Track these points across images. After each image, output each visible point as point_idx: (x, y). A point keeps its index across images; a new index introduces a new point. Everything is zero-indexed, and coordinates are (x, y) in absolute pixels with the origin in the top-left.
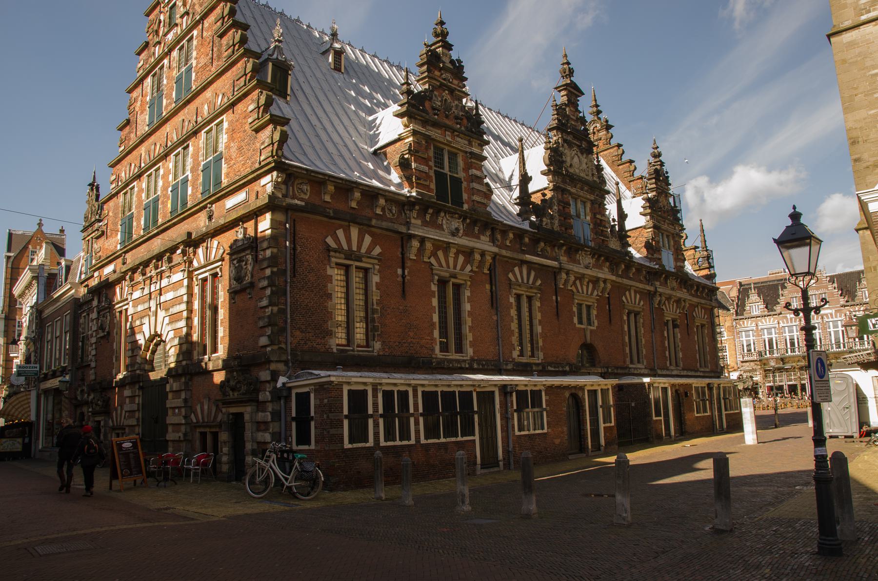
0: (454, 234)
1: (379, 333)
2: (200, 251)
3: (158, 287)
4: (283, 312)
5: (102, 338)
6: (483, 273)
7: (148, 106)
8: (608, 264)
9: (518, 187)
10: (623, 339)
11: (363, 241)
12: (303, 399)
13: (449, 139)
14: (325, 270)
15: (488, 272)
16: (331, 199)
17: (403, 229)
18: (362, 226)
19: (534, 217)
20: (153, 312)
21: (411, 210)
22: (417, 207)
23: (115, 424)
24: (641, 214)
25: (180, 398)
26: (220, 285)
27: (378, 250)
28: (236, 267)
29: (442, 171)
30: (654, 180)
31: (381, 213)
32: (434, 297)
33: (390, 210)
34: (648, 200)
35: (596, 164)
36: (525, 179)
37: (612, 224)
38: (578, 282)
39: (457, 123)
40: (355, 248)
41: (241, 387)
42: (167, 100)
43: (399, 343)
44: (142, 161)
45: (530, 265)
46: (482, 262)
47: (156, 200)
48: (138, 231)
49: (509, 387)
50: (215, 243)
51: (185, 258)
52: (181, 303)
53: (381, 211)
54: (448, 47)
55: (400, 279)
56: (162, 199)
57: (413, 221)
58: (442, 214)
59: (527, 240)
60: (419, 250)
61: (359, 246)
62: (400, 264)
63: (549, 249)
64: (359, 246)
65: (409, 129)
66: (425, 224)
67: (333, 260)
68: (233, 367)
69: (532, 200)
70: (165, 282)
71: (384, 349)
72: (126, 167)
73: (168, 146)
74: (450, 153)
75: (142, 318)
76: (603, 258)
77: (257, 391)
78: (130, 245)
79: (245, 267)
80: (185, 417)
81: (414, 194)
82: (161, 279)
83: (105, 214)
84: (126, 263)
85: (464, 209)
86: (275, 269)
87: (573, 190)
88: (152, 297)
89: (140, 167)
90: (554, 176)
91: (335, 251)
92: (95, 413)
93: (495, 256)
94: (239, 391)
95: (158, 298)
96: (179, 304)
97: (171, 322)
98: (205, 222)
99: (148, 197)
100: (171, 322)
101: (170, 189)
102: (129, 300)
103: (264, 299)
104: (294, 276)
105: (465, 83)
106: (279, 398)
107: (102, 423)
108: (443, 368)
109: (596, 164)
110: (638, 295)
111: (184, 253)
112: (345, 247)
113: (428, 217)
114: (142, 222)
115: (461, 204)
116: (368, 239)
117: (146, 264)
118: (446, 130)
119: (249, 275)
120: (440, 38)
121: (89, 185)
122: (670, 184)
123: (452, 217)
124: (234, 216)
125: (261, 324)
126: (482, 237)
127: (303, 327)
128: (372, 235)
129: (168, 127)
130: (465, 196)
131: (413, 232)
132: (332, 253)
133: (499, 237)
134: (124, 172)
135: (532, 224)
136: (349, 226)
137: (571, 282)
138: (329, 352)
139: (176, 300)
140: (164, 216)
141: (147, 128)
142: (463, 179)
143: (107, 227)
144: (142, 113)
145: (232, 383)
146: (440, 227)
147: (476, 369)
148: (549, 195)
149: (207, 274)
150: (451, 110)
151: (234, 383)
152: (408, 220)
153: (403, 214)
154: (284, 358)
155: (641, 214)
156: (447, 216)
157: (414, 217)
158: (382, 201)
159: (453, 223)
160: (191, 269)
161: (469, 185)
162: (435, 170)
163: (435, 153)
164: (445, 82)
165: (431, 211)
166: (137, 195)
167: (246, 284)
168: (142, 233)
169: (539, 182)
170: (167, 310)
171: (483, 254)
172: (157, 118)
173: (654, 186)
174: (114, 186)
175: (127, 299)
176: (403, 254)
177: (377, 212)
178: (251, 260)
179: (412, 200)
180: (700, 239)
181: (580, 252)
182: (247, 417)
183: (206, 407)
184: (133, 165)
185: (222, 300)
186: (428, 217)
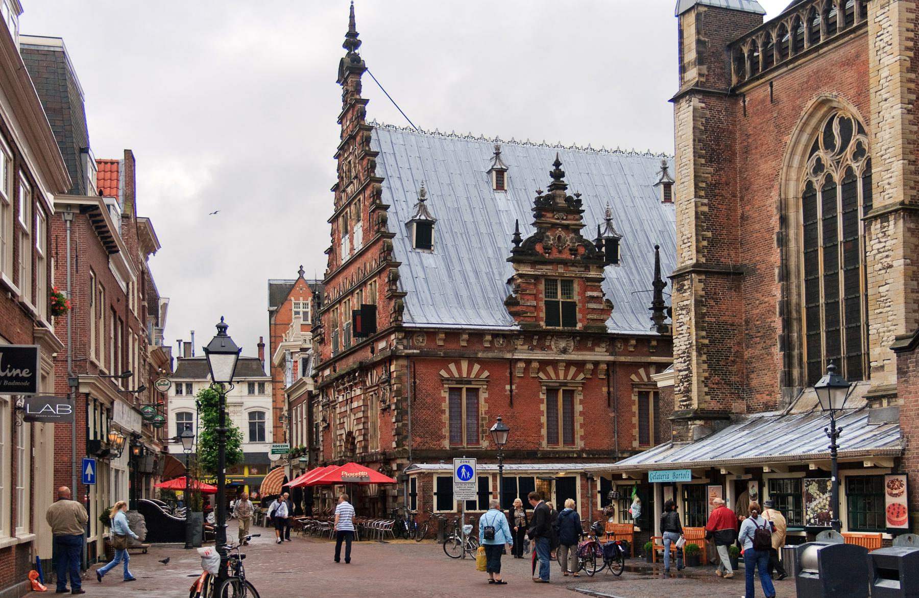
0: (564, 351)
4: (405, 425)
13: (561, 270)
17: (509, 356)
27: (486, 374)
39: (572, 254)
40: (465, 375)
46: (594, 372)
55: (508, 393)
57: (519, 347)
62: (509, 382)
67: (446, 386)
74: (562, 281)
85: (578, 328)
86: (399, 398)
91: (447, 379)
105: (582, 214)
112: (457, 375)
113: (535, 343)
116: (477, 367)
132: (445, 382)
146: (549, 348)
150: (565, 244)
161: (584, 306)
162: (545, 301)
176: (511, 373)
186: (535, 343)
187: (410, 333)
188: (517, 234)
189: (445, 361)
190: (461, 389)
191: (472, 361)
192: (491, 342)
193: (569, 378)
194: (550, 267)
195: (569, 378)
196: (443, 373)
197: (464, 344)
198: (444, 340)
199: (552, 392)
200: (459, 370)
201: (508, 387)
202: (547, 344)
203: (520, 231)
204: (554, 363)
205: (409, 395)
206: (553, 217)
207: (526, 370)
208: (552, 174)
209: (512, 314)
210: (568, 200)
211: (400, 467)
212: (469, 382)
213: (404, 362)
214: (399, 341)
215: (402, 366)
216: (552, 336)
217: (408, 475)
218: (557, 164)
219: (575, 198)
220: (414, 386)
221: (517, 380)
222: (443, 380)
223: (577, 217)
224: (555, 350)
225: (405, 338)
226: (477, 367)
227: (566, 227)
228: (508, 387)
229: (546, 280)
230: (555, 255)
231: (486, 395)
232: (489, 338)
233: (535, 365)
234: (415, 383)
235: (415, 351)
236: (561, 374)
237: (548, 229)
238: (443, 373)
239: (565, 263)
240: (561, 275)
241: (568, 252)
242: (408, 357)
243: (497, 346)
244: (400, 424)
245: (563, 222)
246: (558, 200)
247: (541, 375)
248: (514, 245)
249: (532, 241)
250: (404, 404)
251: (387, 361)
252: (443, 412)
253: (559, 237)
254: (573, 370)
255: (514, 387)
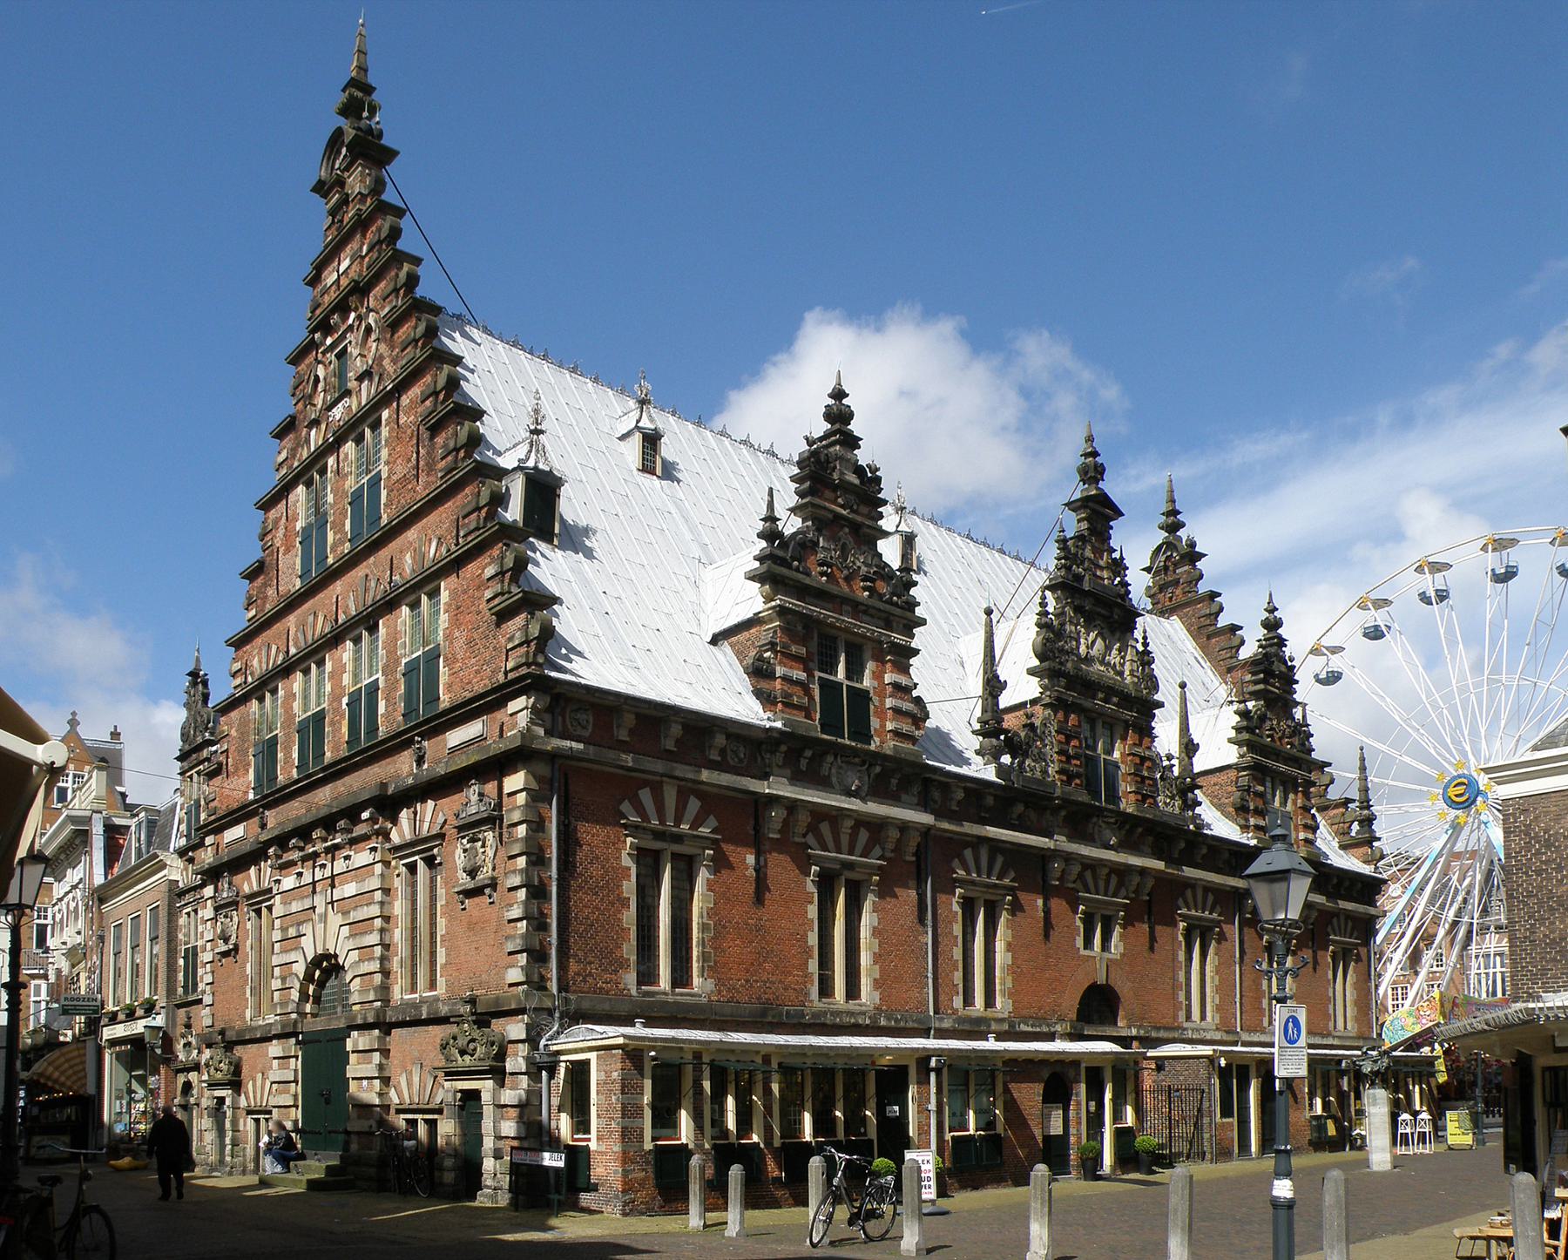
1: (712, 964)
2: (404, 815)
3: (328, 873)
5: (225, 954)
6: (904, 861)
7: (298, 539)
8: (1150, 839)
9: (980, 700)
10: (1174, 978)
11: (685, 807)
12: (579, 1072)
14: (619, 858)
15: (914, 859)
16: (629, 735)
18: (683, 783)
19: (1008, 756)
20: (320, 915)
21: (773, 752)
22: (783, 748)
23: (253, 1104)
24: (1230, 741)
25: (371, 1062)
26: (439, 877)
28: (465, 851)
29: (832, 678)
30: (1262, 675)
31: (719, 759)
32: (811, 902)
33: (735, 753)
34: (1244, 714)
35: (1141, 648)
36: (994, 685)
37: (1166, 763)
38: (1088, 875)
41: (475, 1049)
42: (335, 533)
43: (747, 981)
44: (291, 643)
45: (995, 846)
47: (319, 718)
48: (287, 772)
49: (934, 1059)
50: (430, 803)
51: (376, 827)
52: (370, 904)
53: (719, 755)
54: (852, 442)
55: (751, 872)
56: (332, 716)
58: (830, 759)
59: (990, 801)
60: (786, 822)
63: (1033, 815)
65: (773, 603)
68: (462, 1016)
69: (1005, 725)
70: (340, 866)
71: (720, 992)
72: (260, 650)
73: (340, 621)
75: (299, 924)
76: (1140, 830)
77: (501, 1056)
78: (274, 797)
79: (483, 850)
80: (380, 1095)
81: (779, 724)
82: (333, 860)
83: (223, 732)
84: (266, 825)
85: (873, 747)
87: (1087, 704)
88: (318, 889)
89: (288, 652)
90: (1050, 677)
92: (213, 1085)
93: (927, 831)
94: (472, 1056)
95: (329, 891)
96: (366, 905)
97: (352, 936)
98: (411, 766)
99: (306, 708)
100: (352, 936)
101: (345, 700)
102: (275, 892)
103: (515, 906)
104: (566, 869)
106: (540, 1069)
107: (228, 1101)
108: (824, 1025)
109: (1141, 648)
110: (1210, 894)
111: (373, 820)
113: (803, 764)
114: (295, 755)
115: (868, 738)
116: (694, 805)
117: (303, 832)
118: (842, 603)
119: (490, 865)
120: (837, 426)
121: (189, 674)
122: (1297, 682)
123: (848, 763)
124: (462, 761)
125: (510, 947)
126: (904, 797)
127: (580, 954)
128: (701, 796)
129: (338, 587)
130: (875, 723)
131: (775, 792)
133: (936, 795)
134: (260, 659)
135: (1002, 771)
136: (662, 782)
137: (1073, 876)
138: (623, 993)
139: (363, 897)
140: (336, 748)
141: (298, 584)
142: (871, 692)
143: (227, 758)
144: (288, 551)
145: (462, 1042)
147: (883, 1028)
148: (1040, 713)
149: (416, 857)
151: (465, 1043)
152: (768, 770)
153: (759, 759)
154: (548, 1004)
155: (1230, 741)
156: (839, 761)
157: (777, 765)
158: (720, 740)
159: (849, 773)
160: (387, 846)
163: (820, 645)
164: (844, 512)
165: (808, 753)
166: (283, 703)
167: (484, 879)
168: (295, 774)
169: (1022, 687)
170: (345, 913)
171: (904, 827)
172: (317, 564)
173: (1261, 686)
174: (238, 681)
175: (270, 890)
177: (712, 757)
178: (491, 839)
179: (775, 735)
180: (1357, 784)
181: (1095, 820)
182: (486, 1097)
183: (416, 1079)
184: (274, 648)
185: (444, 903)
186: (803, 764)
207: (786, 825)
209: (758, 694)
229: (821, 636)
233: (803, 819)
242: (554, 757)
243: (731, 762)
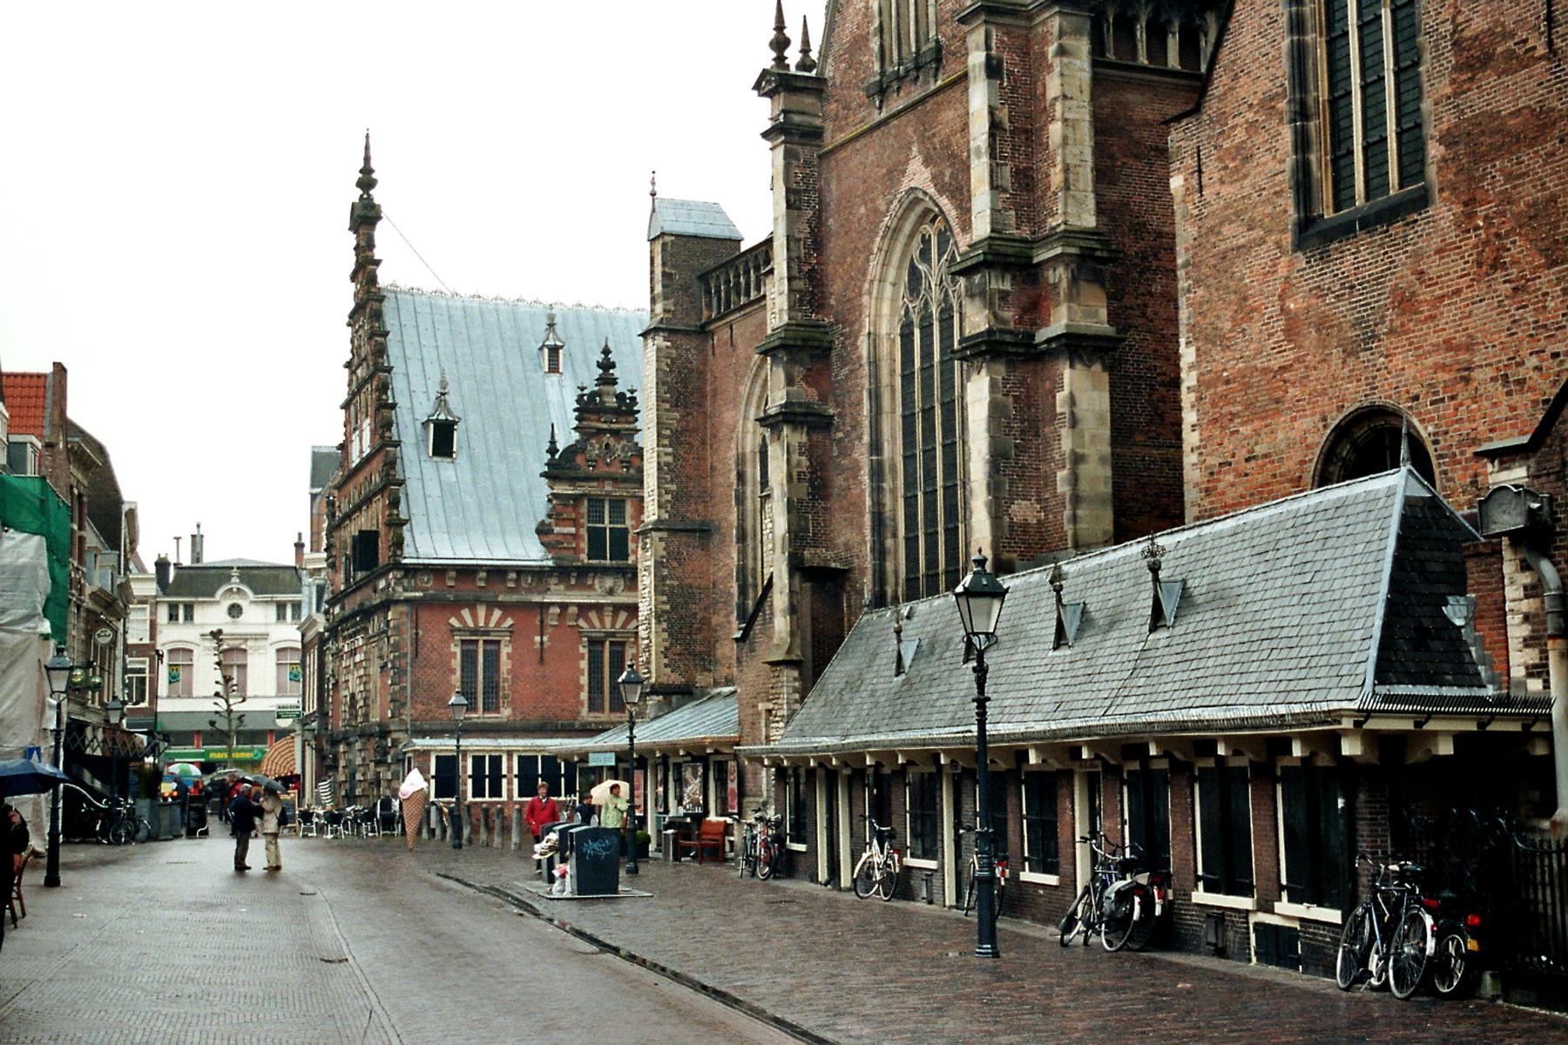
0: (611, 592)
4: (403, 689)
17: (537, 598)
27: (509, 622)
40: (482, 624)
55: (538, 646)
57: (552, 587)
61: (487, 623)
64: (487, 623)
66: (569, 587)
74: (610, 501)
112: (471, 624)
116: (497, 614)
146: (591, 587)
176: (542, 621)
187: (412, 571)
188: (553, 442)
189: (456, 605)
190: (477, 641)
191: (491, 605)
192: (517, 581)
193: (618, 625)
194: (595, 484)
195: (618, 625)
196: (454, 621)
197: (482, 584)
198: (456, 579)
199: (595, 643)
200: (474, 616)
201: (538, 639)
202: (589, 582)
203: (556, 438)
204: (598, 607)
205: (409, 649)
206: (599, 421)
208: (599, 365)
209: (542, 544)
210: (621, 397)
211: (395, 743)
212: (487, 633)
213: (404, 608)
214: (398, 581)
215: (401, 613)
216: (596, 573)
217: (405, 753)
218: (606, 351)
219: (629, 395)
220: (416, 640)
221: (550, 630)
222: (453, 630)
223: (631, 419)
224: (599, 591)
225: (405, 576)
226: (497, 614)
227: (616, 433)
228: (538, 639)
229: (589, 501)
230: (602, 469)
231: (509, 649)
232: (513, 575)
233: (573, 610)
234: (417, 634)
235: (417, 594)
236: (608, 620)
237: (592, 435)
238: (454, 621)
239: (615, 480)
240: (608, 494)
241: (619, 465)
242: (407, 601)
244: (397, 687)
245: (613, 426)
246: (606, 399)
247: (582, 623)
248: (549, 456)
249: (571, 451)
250: (403, 662)
251: (386, 605)
252: (453, 671)
253: (607, 445)
254: (623, 616)
255: (545, 638)
